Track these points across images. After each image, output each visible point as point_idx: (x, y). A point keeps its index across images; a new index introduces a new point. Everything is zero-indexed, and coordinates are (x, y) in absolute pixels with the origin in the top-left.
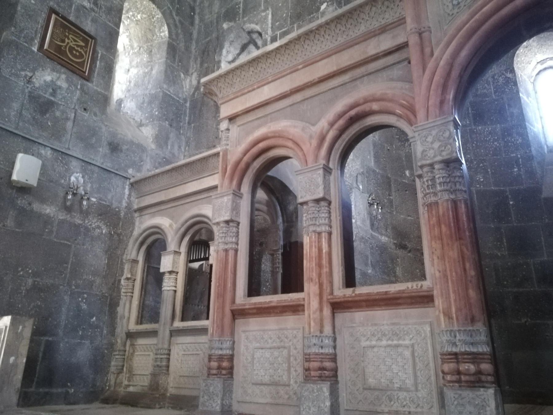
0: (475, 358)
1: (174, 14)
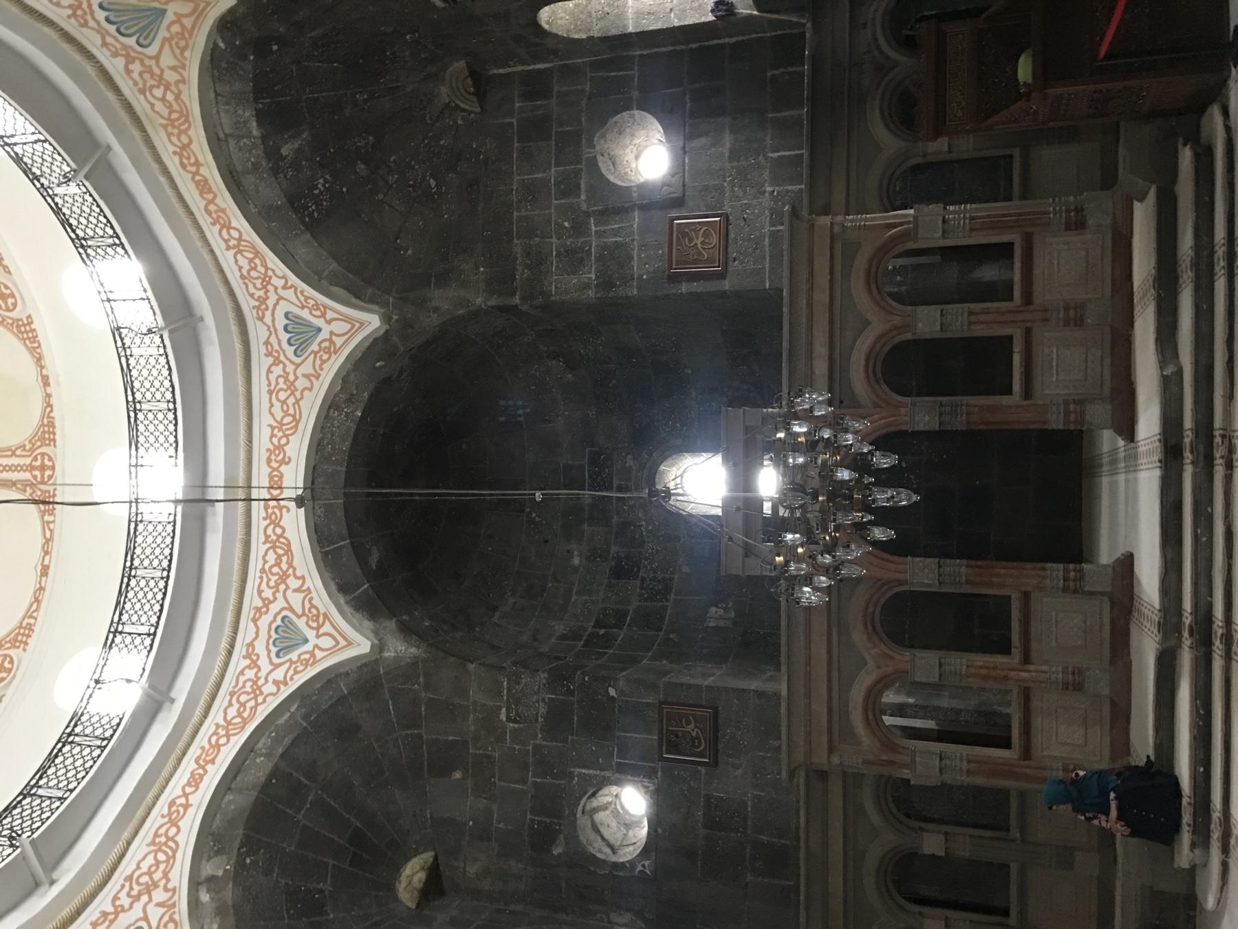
0: (1066, 571)
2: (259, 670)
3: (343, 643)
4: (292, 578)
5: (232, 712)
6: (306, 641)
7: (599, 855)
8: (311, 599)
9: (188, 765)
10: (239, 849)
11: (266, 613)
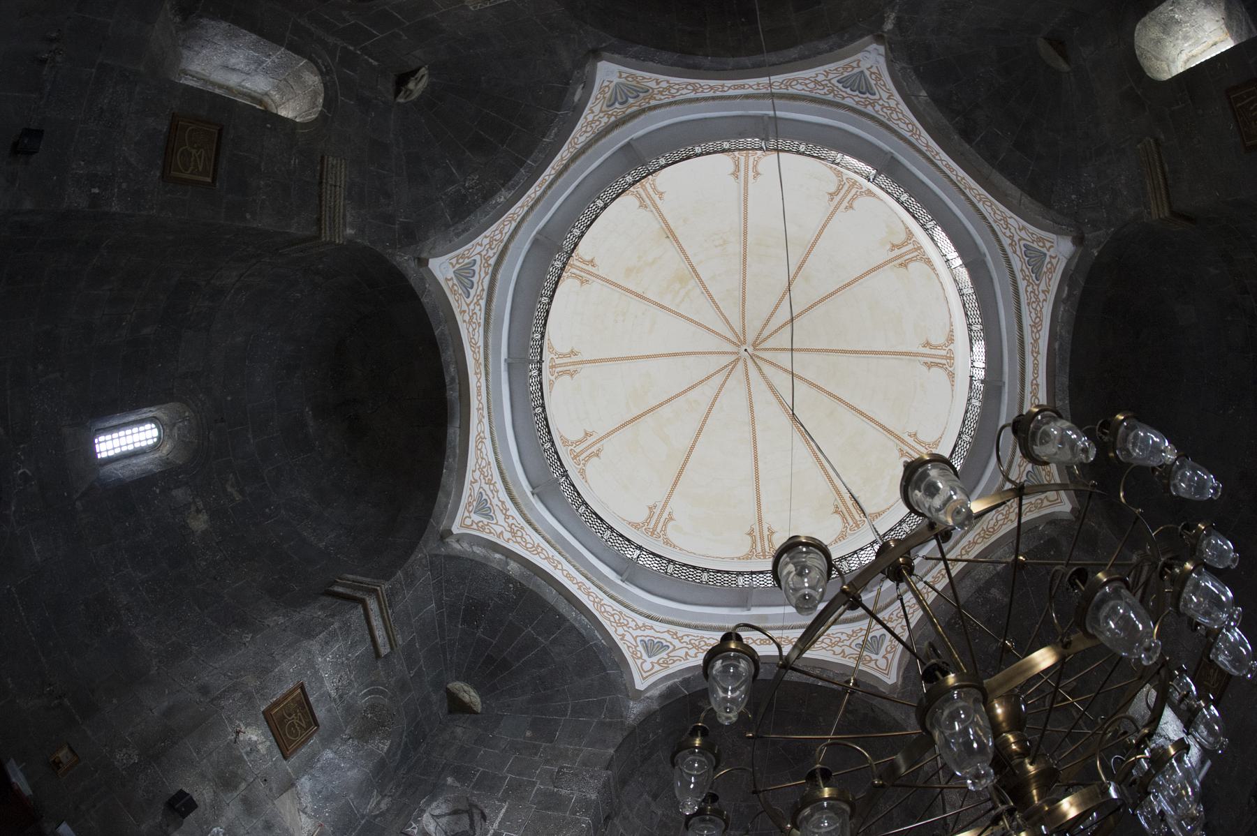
1: (405, 734)
2: (633, 629)
3: (645, 675)
4: (697, 651)
5: (608, 609)
6: (650, 657)
7: (434, 804)
8: (680, 661)
9: (581, 578)
10: (520, 583)
11: (673, 637)
